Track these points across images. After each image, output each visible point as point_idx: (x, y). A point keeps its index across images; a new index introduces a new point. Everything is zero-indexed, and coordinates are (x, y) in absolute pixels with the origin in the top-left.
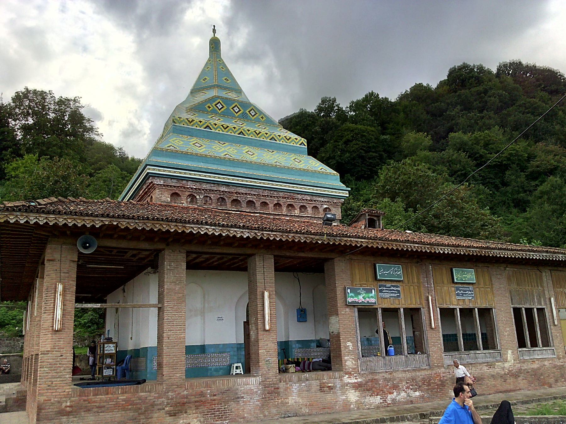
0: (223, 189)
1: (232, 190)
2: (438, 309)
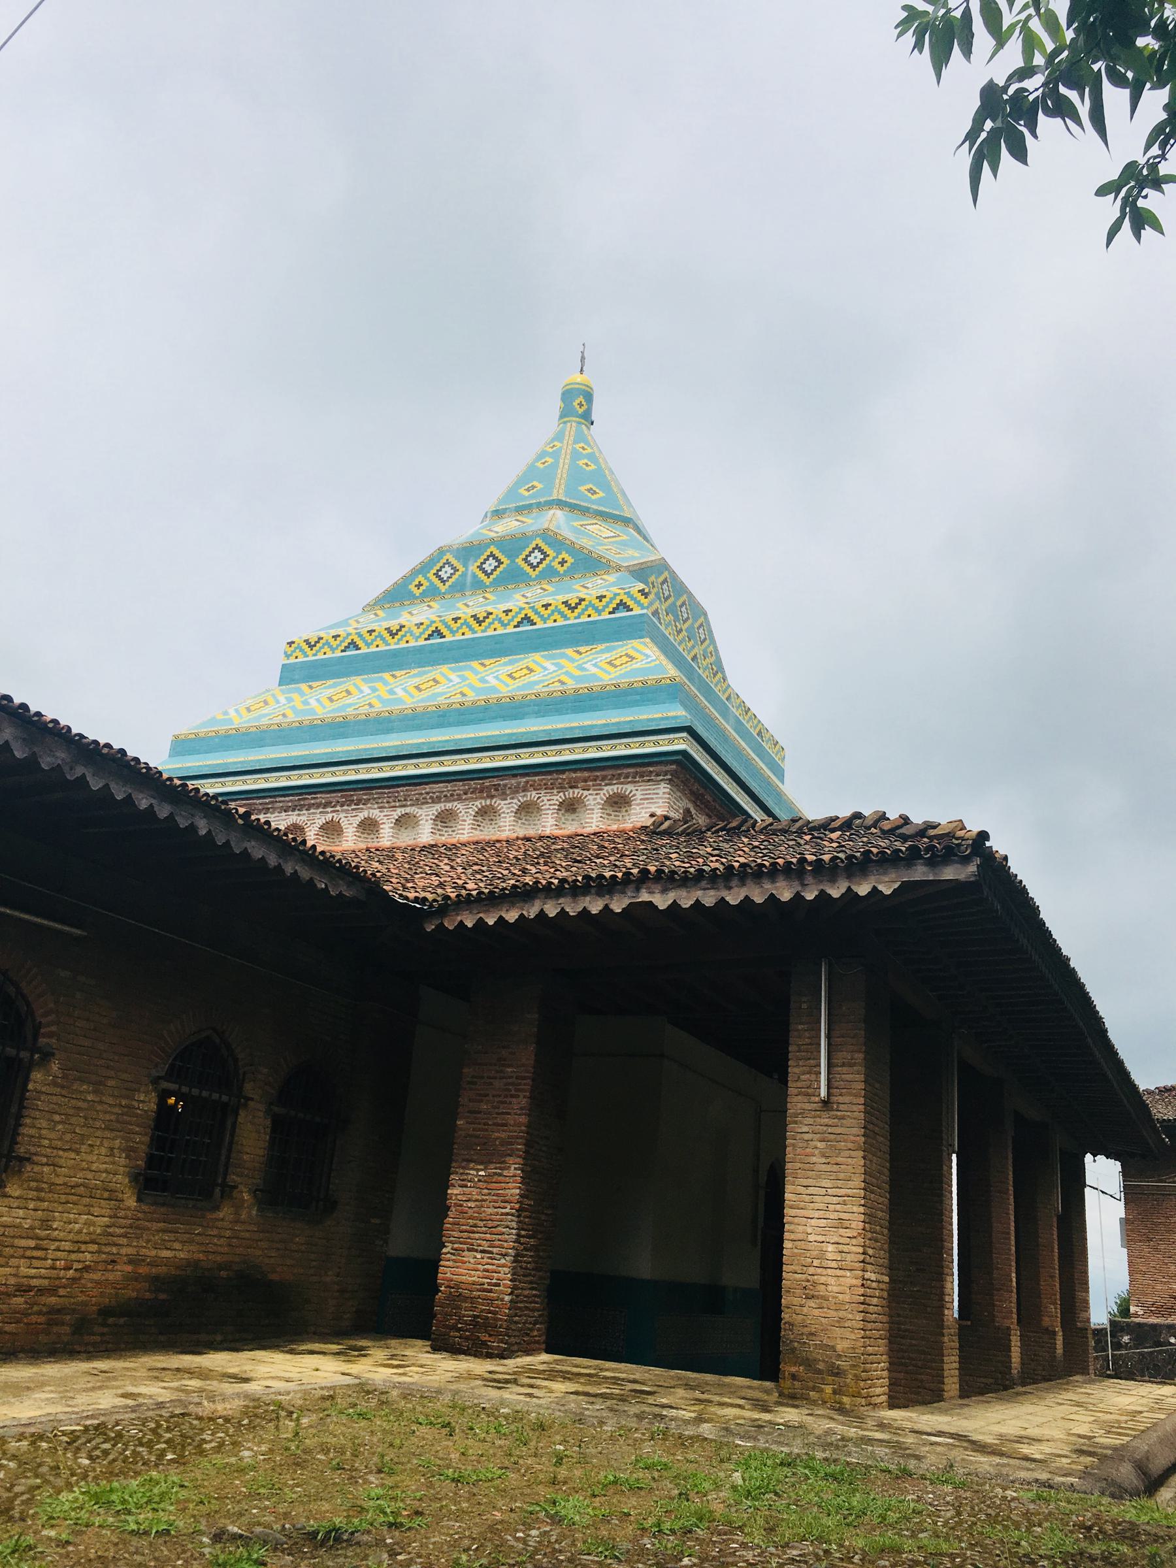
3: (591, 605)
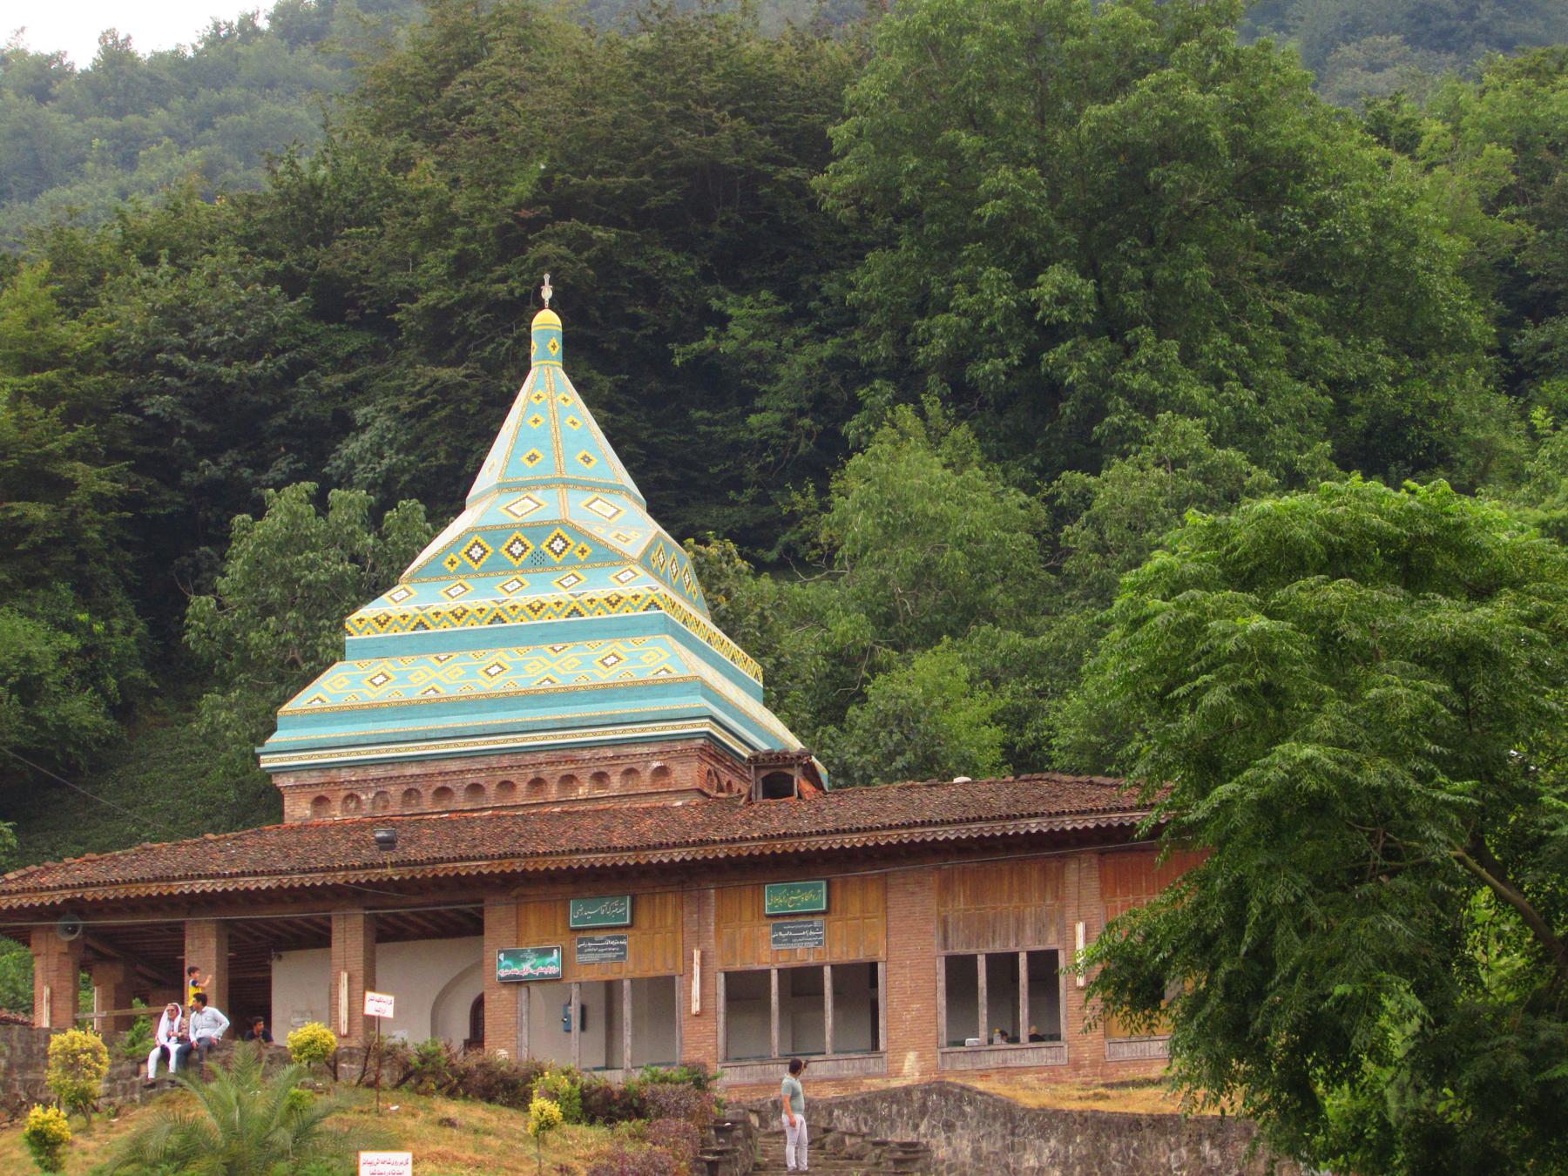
1: (431, 768)
2: (721, 977)
3: (628, 602)
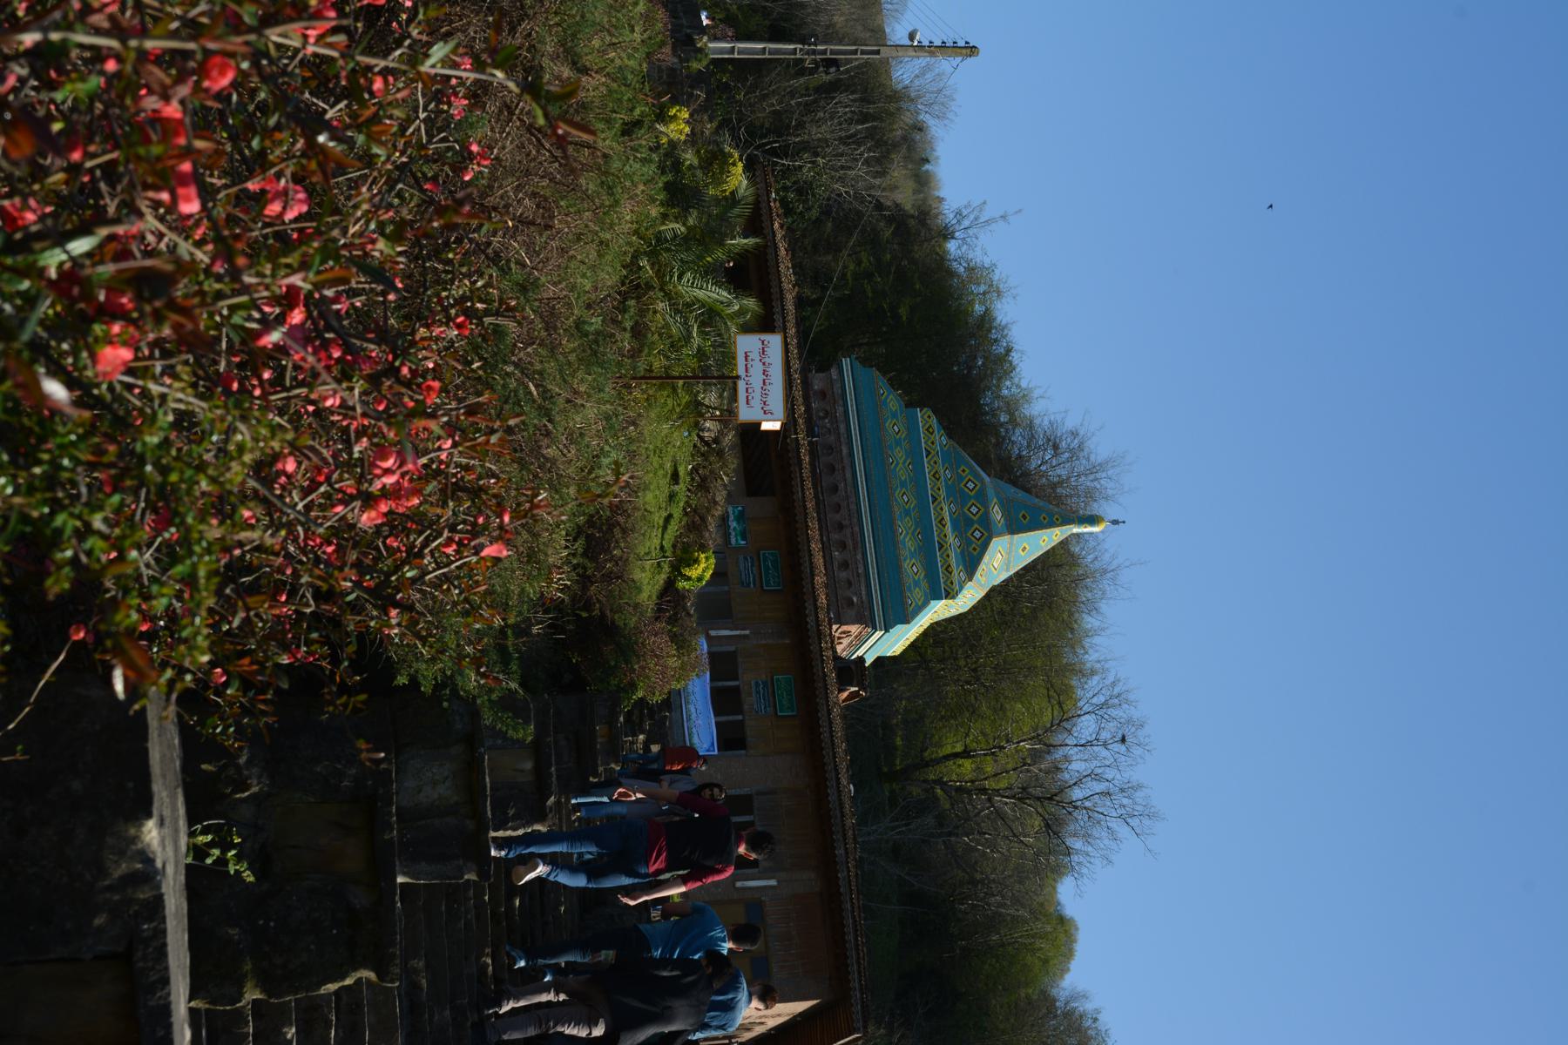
0: (845, 451)
1: (846, 461)
2: (732, 648)
